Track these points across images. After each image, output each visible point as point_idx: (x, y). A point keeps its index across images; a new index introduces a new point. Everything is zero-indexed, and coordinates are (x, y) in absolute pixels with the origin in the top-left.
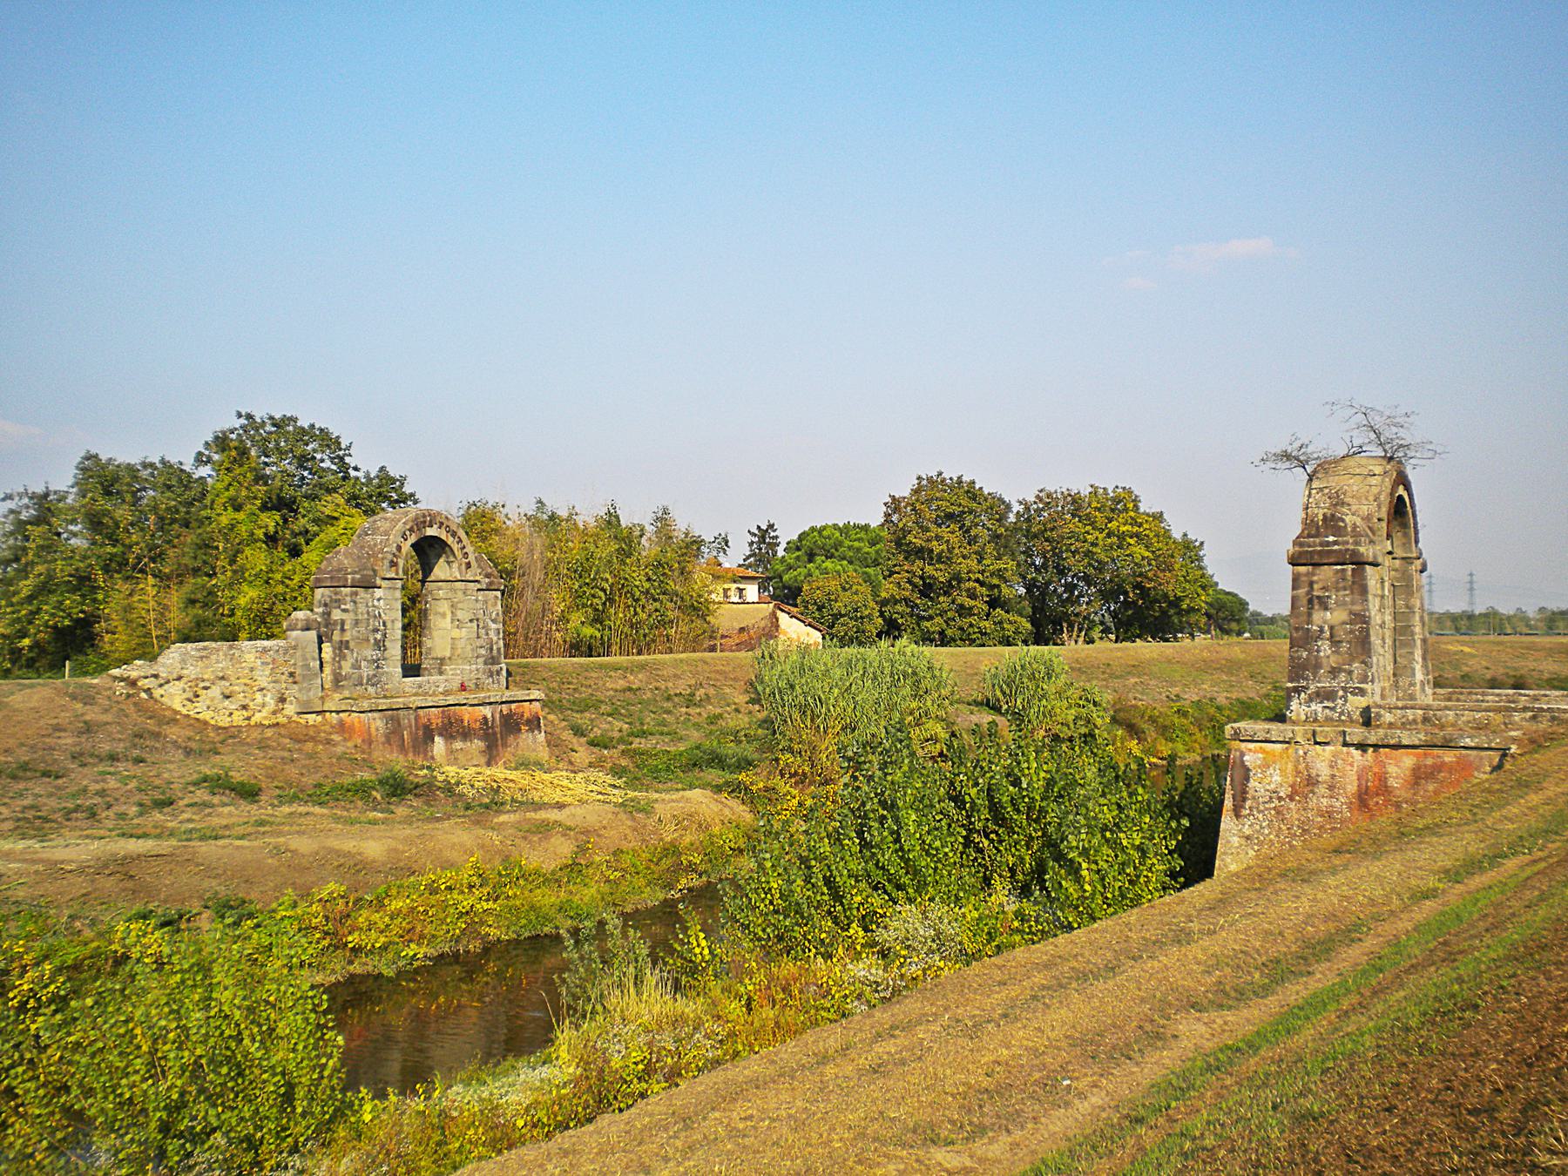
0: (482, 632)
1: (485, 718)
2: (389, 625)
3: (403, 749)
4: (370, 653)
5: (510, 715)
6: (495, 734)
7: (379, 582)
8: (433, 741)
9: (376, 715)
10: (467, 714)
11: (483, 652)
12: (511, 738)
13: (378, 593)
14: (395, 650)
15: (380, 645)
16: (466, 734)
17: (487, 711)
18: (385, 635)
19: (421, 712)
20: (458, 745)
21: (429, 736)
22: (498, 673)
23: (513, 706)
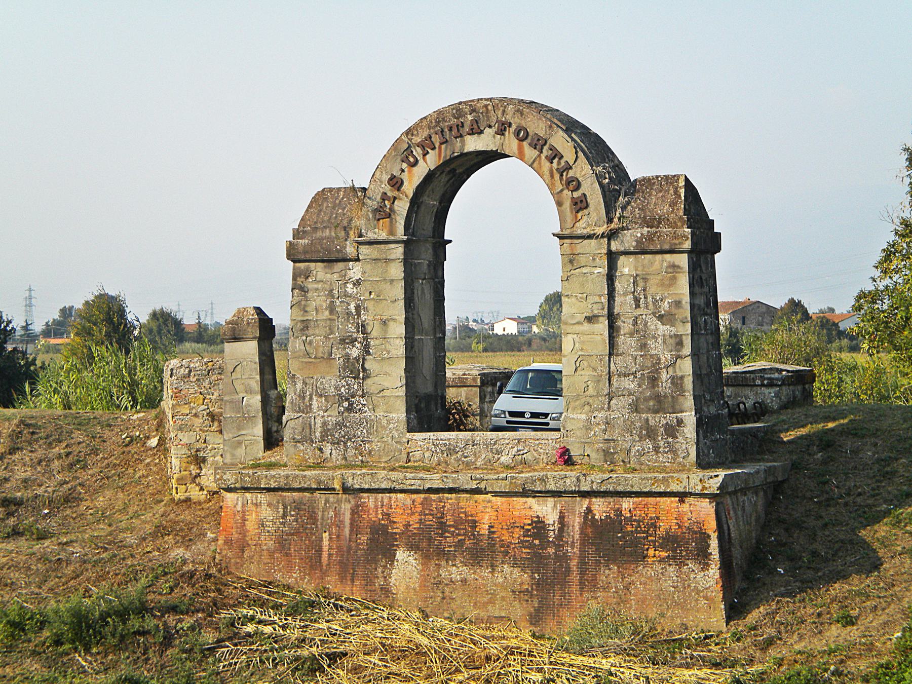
0: (625, 342)
1: (539, 525)
2: (375, 331)
3: (314, 563)
4: (331, 381)
5: (615, 523)
6: (562, 558)
7: (350, 250)
8: (392, 558)
9: (262, 497)
10: (487, 512)
11: (629, 384)
12: (609, 574)
13: (355, 271)
14: (389, 378)
15: (356, 370)
16: (482, 551)
17: (547, 511)
18: (366, 350)
19: (370, 500)
20: (456, 571)
21: (382, 543)
22: (672, 431)
23: (627, 504)
